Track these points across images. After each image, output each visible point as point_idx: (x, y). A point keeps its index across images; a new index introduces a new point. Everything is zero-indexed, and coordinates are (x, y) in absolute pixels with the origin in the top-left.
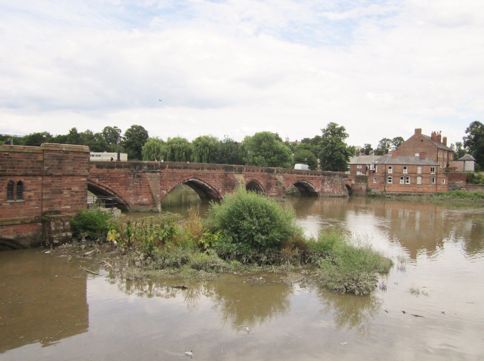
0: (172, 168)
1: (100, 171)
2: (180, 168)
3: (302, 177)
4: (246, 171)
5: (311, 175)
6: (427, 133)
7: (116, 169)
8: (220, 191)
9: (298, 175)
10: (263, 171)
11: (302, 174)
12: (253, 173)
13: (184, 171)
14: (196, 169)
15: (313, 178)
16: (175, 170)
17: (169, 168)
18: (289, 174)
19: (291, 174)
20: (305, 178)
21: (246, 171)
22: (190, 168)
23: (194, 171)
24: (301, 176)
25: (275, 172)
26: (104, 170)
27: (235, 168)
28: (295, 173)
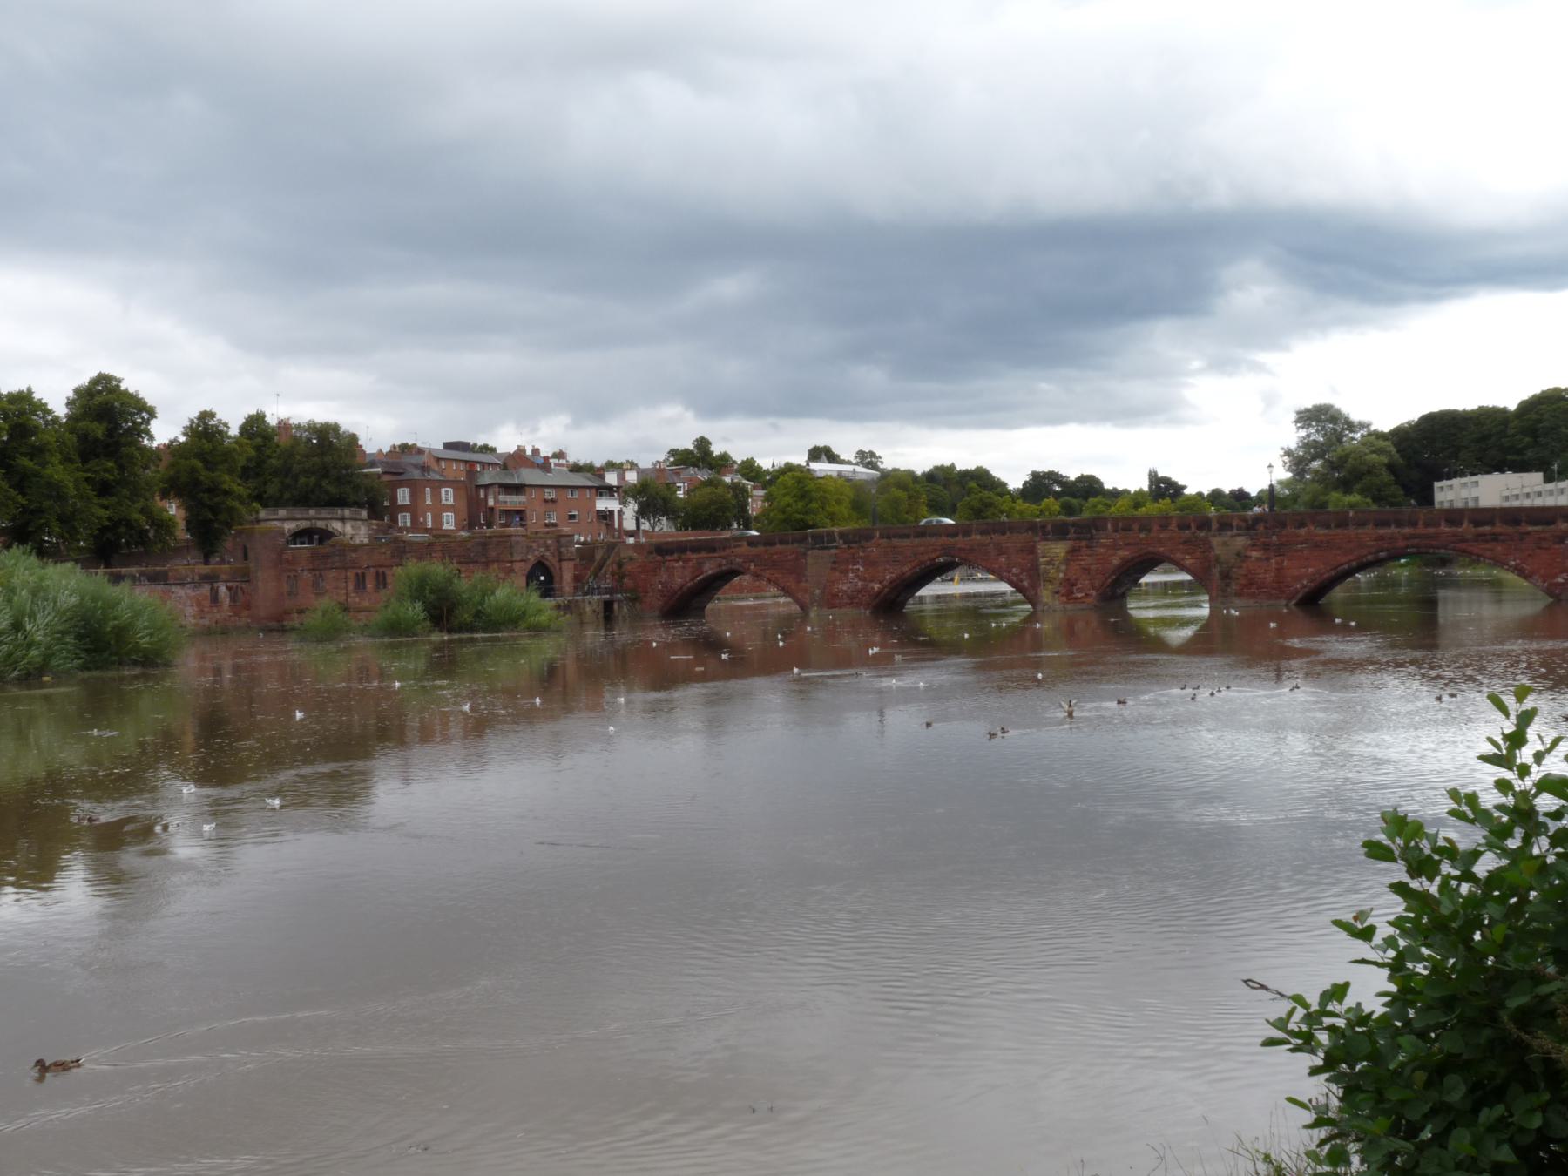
0: (889, 537)
1: (754, 550)
2: (908, 536)
3: (1413, 537)
4: (1116, 531)
5: (1477, 523)
6: (716, 449)
7: (779, 547)
8: (1026, 584)
9: (1382, 531)
10: (1189, 527)
11: (1414, 524)
12: (1142, 535)
13: (917, 541)
14: (948, 535)
15: (1495, 538)
16: (896, 542)
17: (882, 537)
18: (1328, 527)
19: (1338, 526)
20: (1429, 537)
21: (1116, 531)
22: (931, 535)
23: (943, 540)
24: (1406, 530)
25: (1215, 526)
26: (761, 549)
27: (1044, 527)
28: (1362, 524)
